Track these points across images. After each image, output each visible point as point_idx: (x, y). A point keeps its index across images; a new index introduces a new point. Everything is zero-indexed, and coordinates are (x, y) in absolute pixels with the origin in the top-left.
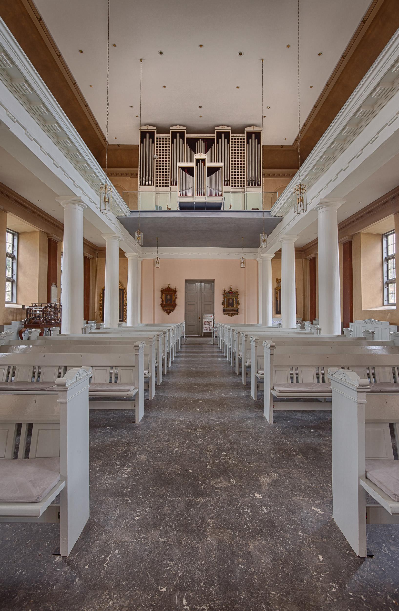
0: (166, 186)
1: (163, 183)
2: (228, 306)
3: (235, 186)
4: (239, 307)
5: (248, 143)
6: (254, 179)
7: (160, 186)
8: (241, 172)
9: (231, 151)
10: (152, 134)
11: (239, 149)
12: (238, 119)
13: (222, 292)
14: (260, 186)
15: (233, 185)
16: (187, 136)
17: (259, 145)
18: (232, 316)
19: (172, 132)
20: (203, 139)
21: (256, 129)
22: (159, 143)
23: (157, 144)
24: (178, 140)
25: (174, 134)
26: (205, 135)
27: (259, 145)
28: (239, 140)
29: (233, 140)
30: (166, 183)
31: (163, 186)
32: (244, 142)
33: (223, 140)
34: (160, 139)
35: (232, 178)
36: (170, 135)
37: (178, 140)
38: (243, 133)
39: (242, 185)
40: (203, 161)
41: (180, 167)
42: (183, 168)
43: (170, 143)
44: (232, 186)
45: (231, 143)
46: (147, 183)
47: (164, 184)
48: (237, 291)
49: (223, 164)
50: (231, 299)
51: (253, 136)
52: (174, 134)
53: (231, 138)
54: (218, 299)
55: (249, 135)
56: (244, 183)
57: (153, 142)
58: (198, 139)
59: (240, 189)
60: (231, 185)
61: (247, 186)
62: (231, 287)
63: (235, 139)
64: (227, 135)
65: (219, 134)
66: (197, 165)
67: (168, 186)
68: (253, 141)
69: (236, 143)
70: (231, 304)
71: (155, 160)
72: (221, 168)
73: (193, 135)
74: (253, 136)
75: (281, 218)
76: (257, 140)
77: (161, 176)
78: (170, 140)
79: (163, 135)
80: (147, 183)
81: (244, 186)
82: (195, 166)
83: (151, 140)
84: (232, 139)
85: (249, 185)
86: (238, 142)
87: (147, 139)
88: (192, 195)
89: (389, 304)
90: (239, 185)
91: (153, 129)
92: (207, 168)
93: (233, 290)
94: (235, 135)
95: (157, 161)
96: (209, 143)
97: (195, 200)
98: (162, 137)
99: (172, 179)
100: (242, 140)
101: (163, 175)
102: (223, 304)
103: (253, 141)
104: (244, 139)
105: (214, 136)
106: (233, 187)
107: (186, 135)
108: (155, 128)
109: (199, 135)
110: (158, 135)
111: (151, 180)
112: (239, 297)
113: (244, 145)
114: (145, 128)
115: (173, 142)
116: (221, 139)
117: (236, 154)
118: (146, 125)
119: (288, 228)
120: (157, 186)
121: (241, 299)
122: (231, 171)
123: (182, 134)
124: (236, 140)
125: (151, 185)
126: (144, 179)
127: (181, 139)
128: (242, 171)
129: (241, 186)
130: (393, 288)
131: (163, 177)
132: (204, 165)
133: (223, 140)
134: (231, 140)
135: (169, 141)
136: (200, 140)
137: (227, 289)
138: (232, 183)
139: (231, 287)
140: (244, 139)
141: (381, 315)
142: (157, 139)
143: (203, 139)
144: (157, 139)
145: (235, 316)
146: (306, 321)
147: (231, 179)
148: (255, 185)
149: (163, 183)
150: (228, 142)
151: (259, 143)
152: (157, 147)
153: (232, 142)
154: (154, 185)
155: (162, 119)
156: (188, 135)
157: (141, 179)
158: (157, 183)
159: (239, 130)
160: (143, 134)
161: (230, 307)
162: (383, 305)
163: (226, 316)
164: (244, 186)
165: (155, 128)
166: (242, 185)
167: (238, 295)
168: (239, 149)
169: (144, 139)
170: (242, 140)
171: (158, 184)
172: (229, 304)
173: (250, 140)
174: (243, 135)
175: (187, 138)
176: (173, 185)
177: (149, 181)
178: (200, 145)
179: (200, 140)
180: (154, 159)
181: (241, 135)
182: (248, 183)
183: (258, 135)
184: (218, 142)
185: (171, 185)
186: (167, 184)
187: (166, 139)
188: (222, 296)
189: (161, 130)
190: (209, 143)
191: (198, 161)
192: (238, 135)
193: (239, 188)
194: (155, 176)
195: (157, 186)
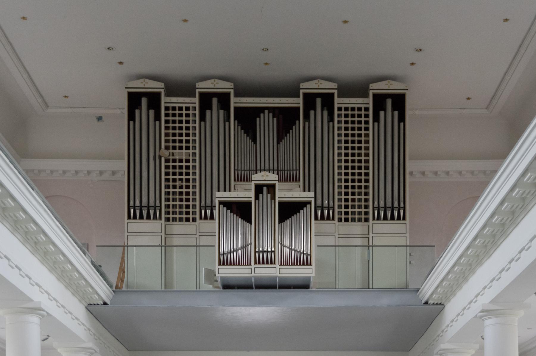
0: (188, 220)
1: (181, 213)
3: (346, 220)
5: (376, 119)
7: (174, 220)
9: (336, 138)
10: (154, 100)
11: (356, 126)
12: (352, 69)
14: (404, 219)
15: (343, 217)
16: (235, 102)
17: (402, 124)
20: (275, 111)
22: (171, 118)
23: (167, 122)
24: (215, 113)
25: (206, 100)
26: (277, 100)
27: (402, 124)
28: (356, 112)
29: (343, 112)
30: (188, 213)
31: (181, 220)
32: (367, 116)
33: (319, 114)
34: (174, 108)
35: (340, 200)
36: (196, 100)
37: (215, 113)
38: (366, 96)
39: (363, 217)
40: (271, 188)
41: (220, 203)
42: (228, 205)
43: (197, 119)
44: (340, 220)
45: (336, 119)
46: (145, 213)
47: (184, 216)
49: (312, 194)
52: (206, 100)
53: (336, 106)
55: (379, 101)
56: (366, 213)
57: (157, 118)
58: (261, 110)
59: (356, 228)
60: (337, 217)
61: (374, 219)
63: (346, 109)
64: (328, 100)
65: (310, 100)
66: (257, 198)
67: (194, 220)
68: (389, 114)
69: (350, 119)
71: (163, 160)
72: (310, 203)
78: (197, 112)
79: (181, 99)
80: (145, 213)
82: (253, 200)
83: (152, 112)
85: (379, 219)
86: (353, 116)
87: (144, 112)
88: (248, 263)
90: (357, 217)
92: (280, 203)
94: (346, 100)
95: (167, 161)
96: (286, 119)
97: (253, 274)
98: (177, 105)
99: (203, 204)
100: (363, 113)
101: (181, 193)
103: (389, 114)
104: (367, 109)
105: (298, 102)
106: (343, 223)
107: (233, 100)
108: (162, 85)
109: (264, 100)
110: (169, 99)
111: (155, 207)
113: (367, 122)
114: (139, 86)
115: (203, 118)
116: (315, 109)
117: (350, 138)
118: (140, 77)
120: (168, 220)
122: (337, 184)
123: (224, 99)
124: (350, 112)
128: (363, 184)
129: (360, 220)
131: (181, 200)
132: (273, 198)
133: (319, 114)
134: (336, 112)
135: (195, 115)
138: (340, 213)
140: (367, 109)
142: (167, 108)
144: (167, 108)
147: (337, 203)
150: (331, 119)
153: (339, 116)
154: (160, 218)
155: (179, 67)
156: (238, 99)
158: (168, 213)
160: (134, 100)
165: (162, 85)
166: (363, 217)
168: (356, 126)
169: (137, 112)
170: (363, 113)
171: (171, 216)
173: (382, 113)
174: (365, 100)
175: (235, 108)
176: (206, 218)
177: (148, 207)
178: (267, 125)
180: (160, 157)
182: (376, 212)
184: (307, 117)
185: (201, 218)
186: (191, 216)
187: (187, 109)
189: (176, 88)
190: (286, 119)
191: (259, 189)
193: (357, 223)
194: (163, 197)
195: (168, 220)
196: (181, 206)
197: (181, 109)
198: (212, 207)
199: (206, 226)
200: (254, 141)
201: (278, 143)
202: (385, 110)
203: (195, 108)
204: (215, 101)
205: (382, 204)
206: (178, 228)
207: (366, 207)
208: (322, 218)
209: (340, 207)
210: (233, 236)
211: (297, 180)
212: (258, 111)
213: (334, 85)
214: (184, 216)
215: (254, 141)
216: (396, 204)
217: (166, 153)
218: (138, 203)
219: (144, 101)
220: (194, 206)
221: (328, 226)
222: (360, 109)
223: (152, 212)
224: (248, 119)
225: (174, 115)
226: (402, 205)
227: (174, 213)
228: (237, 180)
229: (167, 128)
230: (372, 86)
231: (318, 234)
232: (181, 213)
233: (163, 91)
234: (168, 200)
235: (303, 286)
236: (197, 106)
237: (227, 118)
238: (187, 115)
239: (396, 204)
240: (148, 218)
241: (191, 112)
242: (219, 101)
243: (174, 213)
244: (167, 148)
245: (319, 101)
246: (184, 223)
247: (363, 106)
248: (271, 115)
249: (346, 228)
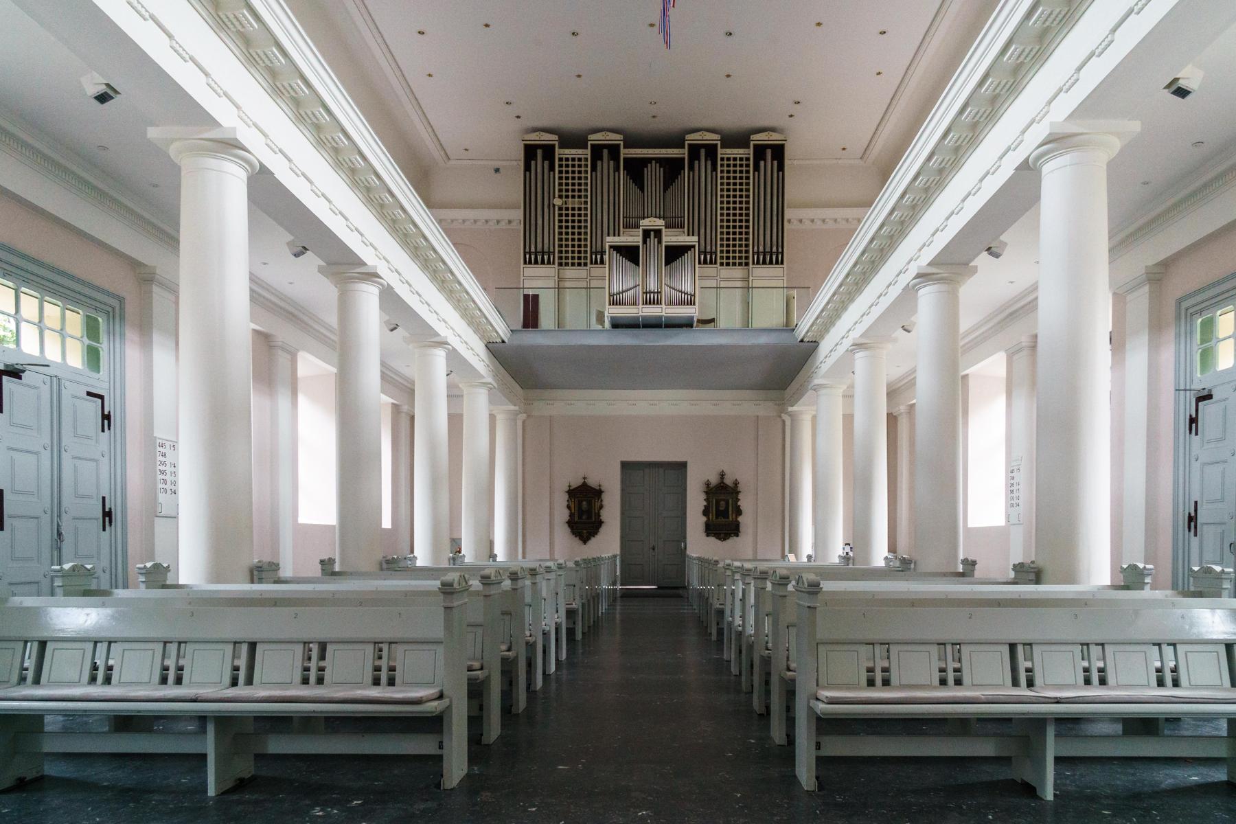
0: (579, 264)
1: (573, 258)
3: (728, 264)
4: (740, 519)
5: (757, 168)
6: (768, 249)
7: (567, 264)
10: (548, 151)
12: (733, 120)
13: (703, 488)
16: (624, 153)
19: (592, 146)
20: (661, 161)
21: (774, 138)
23: (560, 172)
24: (606, 164)
25: (597, 151)
26: (664, 151)
30: (579, 258)
31: (573, 264)
32: (748, 166)
33: (703, 164)
34: (567, 160)
36: (589, 151)
37: (606, 164)
38: (748, 147)
40: (658, 233)
41: (611, 247)
44: (722, 264)
45: (719, 169)
46: (539, 258)
48: (736, 483)
49: (695, 238)
50: (722, 503)
51: (769, 152)
53: (719, 156)
54: (695, 502)
55: (760, 151)
56: (747, 258)
57: (552, 168)
58: (649, 160)
59: (737, 272)
62: (722, 475)
63: (728, 159)
64: (711, 150)
65: (694, 150)
66: (645, 242)
67: (585, 265)
68: (769, 163)
70: (724, 513)
74: (769, 152)
75: (815, 344)
76: (775, 162)
80: (539, 258)
81: (747, 264)
82: (641, 244)
83: (546, 163)
84: (722, 159)
87: (539, 163)
88: (636, 304)
91: (552, 139)
92: (666, 247)
93: (728, 481)
94: (729, 151)
95: (560, 209)
96: (672, 169)
101: (573, 240)
102: (706, 512)
103: (769, 163)
104: (748, 159)
105: (684, 153)
107: (623, 151)
108: (555, 137)
110: (562, 151)
112: (741, 496)
113: (748, 172)
114: (535, 138)
115: (594, 168)
118: (535, 130)
119: (830, 362)
120: (560, 264)
121: (745, 502)
123: (614, 150)
126: (533, 249)
129: (740, 264)
132: (660, 242)
133: (703, 164)
134: (719, 162)
137: (714, 480)
138: (722, 258)
139: (722, 475)
144: (560, 159)
148: (771, 263)
150: (714, 168)
153: (722, 165)
155: (572, 120)
156: (627, 151)
158: (560, 258)
159: (738, 139)
160: (530, 151)
161: (722, 520)
163: (712, 539)
165: (556, 137)
167: (738, 493)
169: (533, 163)
172: (719, 514)
173: (762, 163)
177: (543, 253)
178: (654, 175)
181: (741, 151)
184: (691, 168)
187: (580, 160)
188: (703, 496)
190: (672, 169)
191: (646, 234)
192: (735, 151)
196: (573, 252)
197: (573, 160)
198: (603, 253)
199: (596, 270)
200: (642, 190)
202: (765, 160)
204: (605, 152)
205: (761, 249)
206: (570, 272)
207: (747, 252)
208: (705, 262)
209: (722, 252)
210: (621, 279)
211: (682, 226)
212: (645, 161)
213: (717, 137)
215: (642, 190)
216: (774, 249)
217: (558, 202)
218: (533, 249)
219: (539, 152)
220: (586, 252)
221: (710, 270)
222: (741, 159)
224: (636, 169)
225: (567, 166)
227: (567, 258)
228: (625, 227)
229: (560, 178)
230: (754, 137)
231: (701, 278)
232: (573, 258)
234: (560, 246)
235: (686, 324)
237: (617, 169)
238: (580, 166)
239: (774, 249)
240: (543, 262)
242: (609, 153)
243: (567, 258)
244: (560, 197)
245: (703, 152)
249: (726, 272)
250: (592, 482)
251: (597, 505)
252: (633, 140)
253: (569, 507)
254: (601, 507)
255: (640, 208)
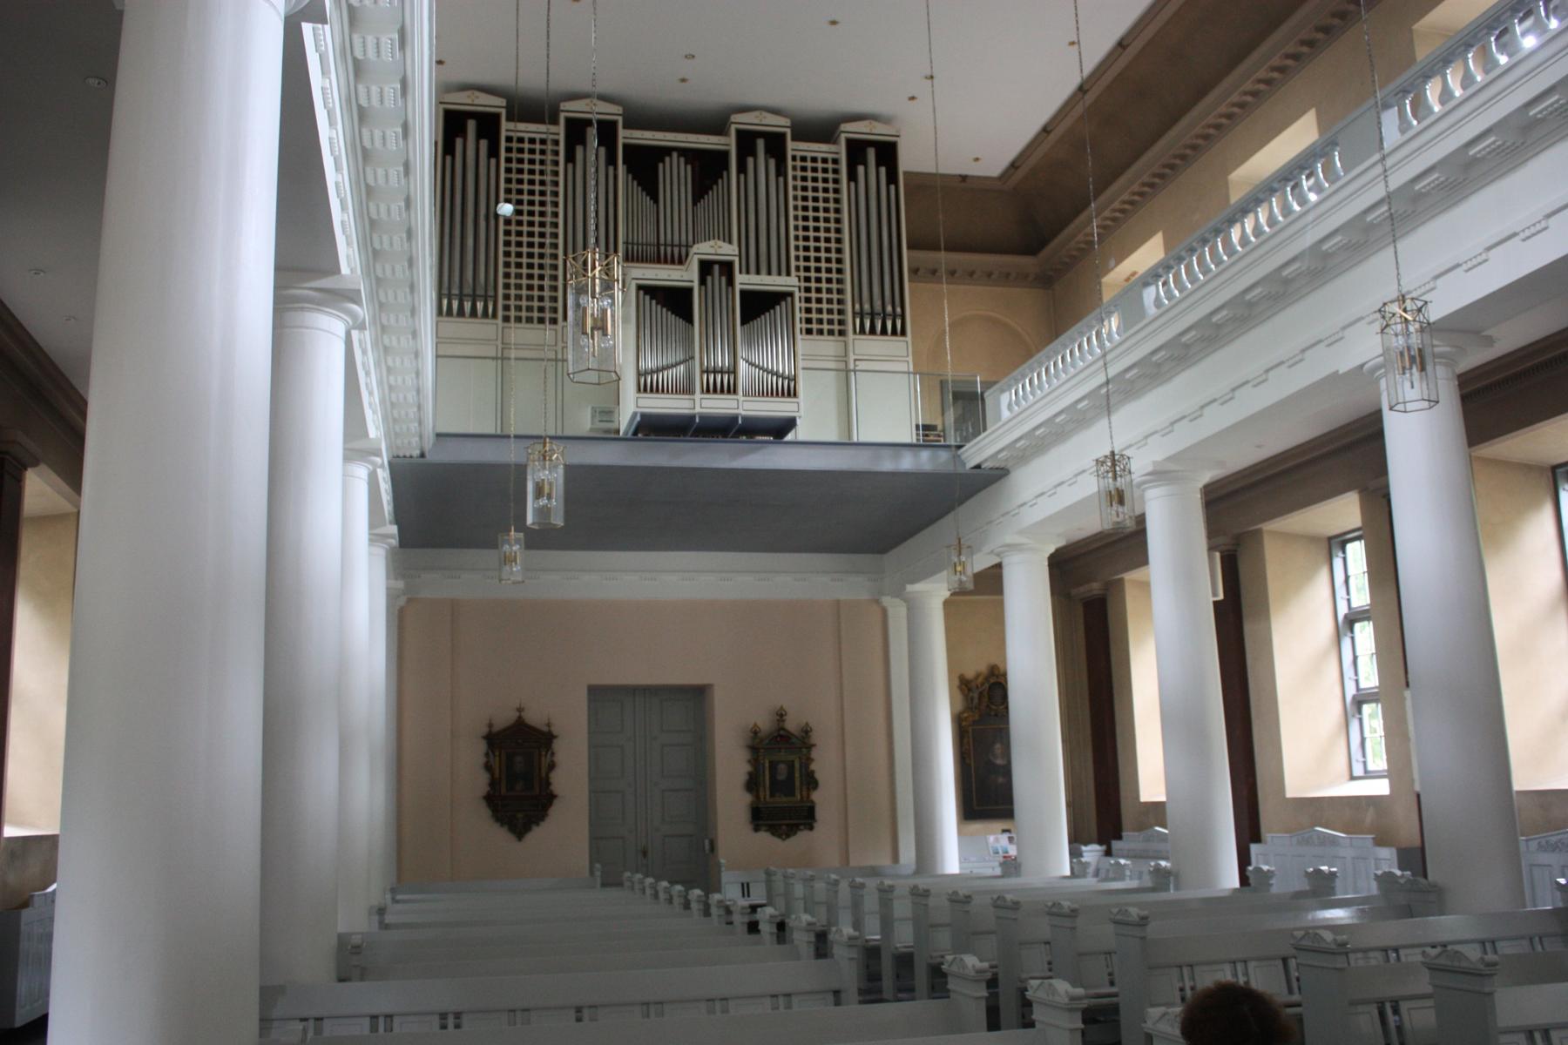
2: (772, 795)
8: (829, 281)
10: (488, 125)
16: (624, 136)
18: (788, 836)
19: (568, 120)
20: (689, 155)
23: (509, 160)
25: (577, 130)
26: (692, 137)
27: (892, 187)
31: (529, 320)
33: (761, 161)
34: (521, 140)
36: (560, 131)
46: (468, 306)
51: (871, 154)
52: (577, 130)
53: (790, 154)
55: (857, 149)
56: (841, 322)
57: (493, 152)
58: (667, 151)
59: (827, 346)
63: (804, 159)
64: (776, 144)
65: (747, 140)
68: (871, 171)
73: (648, 134)
76: (883, 170)
77: (524, 282)
78: (562, 148)
80: (468, 306)
83: (484, 144)
89: (1368, 775)
91: (494, 104)
96: (708, 169)
100: (830, 166)
103: (871, 171)
105: (730, 143)
108: (502, 102)
114: (464, 101)
115: (570, 158)
116: (754, 155)
120: (506, 319)
123: (607, 131)
125: (485, 314)
127: (602, 150)
129: (831, 332)
130: (1373, 716)
133: (761, 161)
136: (675, 155)
140: (835, 161)
141: (1350, 812)
143: (683, 152)
144: (509, 139)
145: (802, 837)
146: (1086, 844)
149: (530, 309)
151: (892, 178)
152: (508, 170)
156: (629, 133)
157: (445, 291)
158: (507, 308)
159: (820, 129)
160: (453, 124)
162: (1352, 778)
164: (842, 333)
165: (502, 102)
166: (836, 327)
169: (459, 141)
173: (861, 169)
175: (625, 146)
178: (675, 178)
179: (675, 155)
181: (824, 147)
183: (887, 153)
190: (708, 169)
193: (825, 337)
197: (532, 141)
200: (655, 199)
201: (695, 204)
202: (865, 164)
203: (556, 143)
212: (663, 152)
214: (536, 314)
215: (655, 199)
219: (471, 125)
222: (825, 161)
223: (480, 306)
224: (644, 165)
225: (521, 151)
226: (899, 310)
230: (845, 127)
233: (504, 112)
236: (562, 138)
237: (611, 160)
239: (889, 309)
241: (549, 147)
246: (536, 325)
247: (830, 156)
248: (682, 160)
250: (534, 718)
251: (545, 762)
252: (637, 118)
253: (488, 767)
254: (552, 766)
255: (652, 227)
